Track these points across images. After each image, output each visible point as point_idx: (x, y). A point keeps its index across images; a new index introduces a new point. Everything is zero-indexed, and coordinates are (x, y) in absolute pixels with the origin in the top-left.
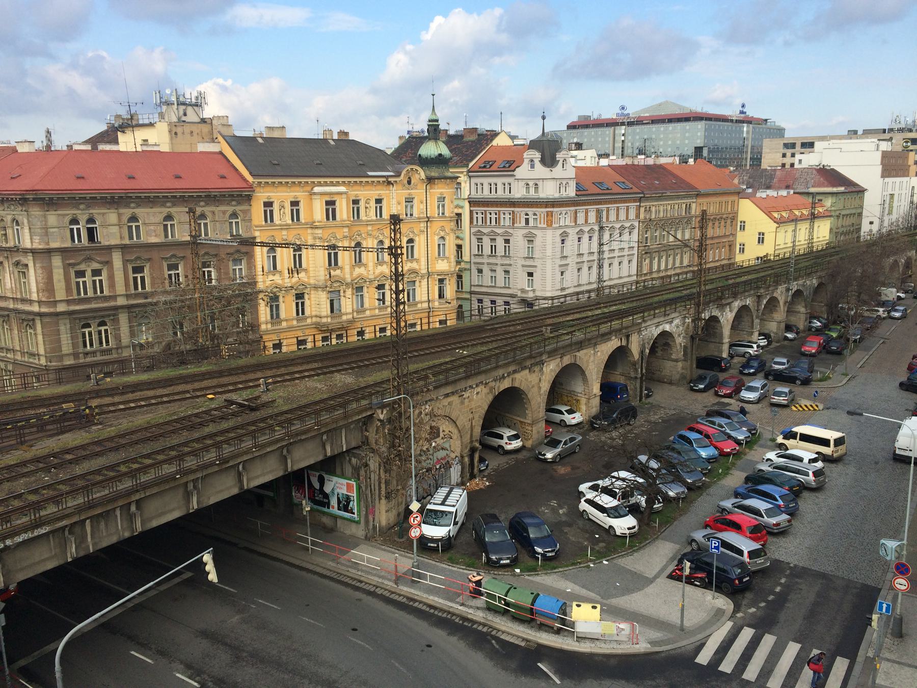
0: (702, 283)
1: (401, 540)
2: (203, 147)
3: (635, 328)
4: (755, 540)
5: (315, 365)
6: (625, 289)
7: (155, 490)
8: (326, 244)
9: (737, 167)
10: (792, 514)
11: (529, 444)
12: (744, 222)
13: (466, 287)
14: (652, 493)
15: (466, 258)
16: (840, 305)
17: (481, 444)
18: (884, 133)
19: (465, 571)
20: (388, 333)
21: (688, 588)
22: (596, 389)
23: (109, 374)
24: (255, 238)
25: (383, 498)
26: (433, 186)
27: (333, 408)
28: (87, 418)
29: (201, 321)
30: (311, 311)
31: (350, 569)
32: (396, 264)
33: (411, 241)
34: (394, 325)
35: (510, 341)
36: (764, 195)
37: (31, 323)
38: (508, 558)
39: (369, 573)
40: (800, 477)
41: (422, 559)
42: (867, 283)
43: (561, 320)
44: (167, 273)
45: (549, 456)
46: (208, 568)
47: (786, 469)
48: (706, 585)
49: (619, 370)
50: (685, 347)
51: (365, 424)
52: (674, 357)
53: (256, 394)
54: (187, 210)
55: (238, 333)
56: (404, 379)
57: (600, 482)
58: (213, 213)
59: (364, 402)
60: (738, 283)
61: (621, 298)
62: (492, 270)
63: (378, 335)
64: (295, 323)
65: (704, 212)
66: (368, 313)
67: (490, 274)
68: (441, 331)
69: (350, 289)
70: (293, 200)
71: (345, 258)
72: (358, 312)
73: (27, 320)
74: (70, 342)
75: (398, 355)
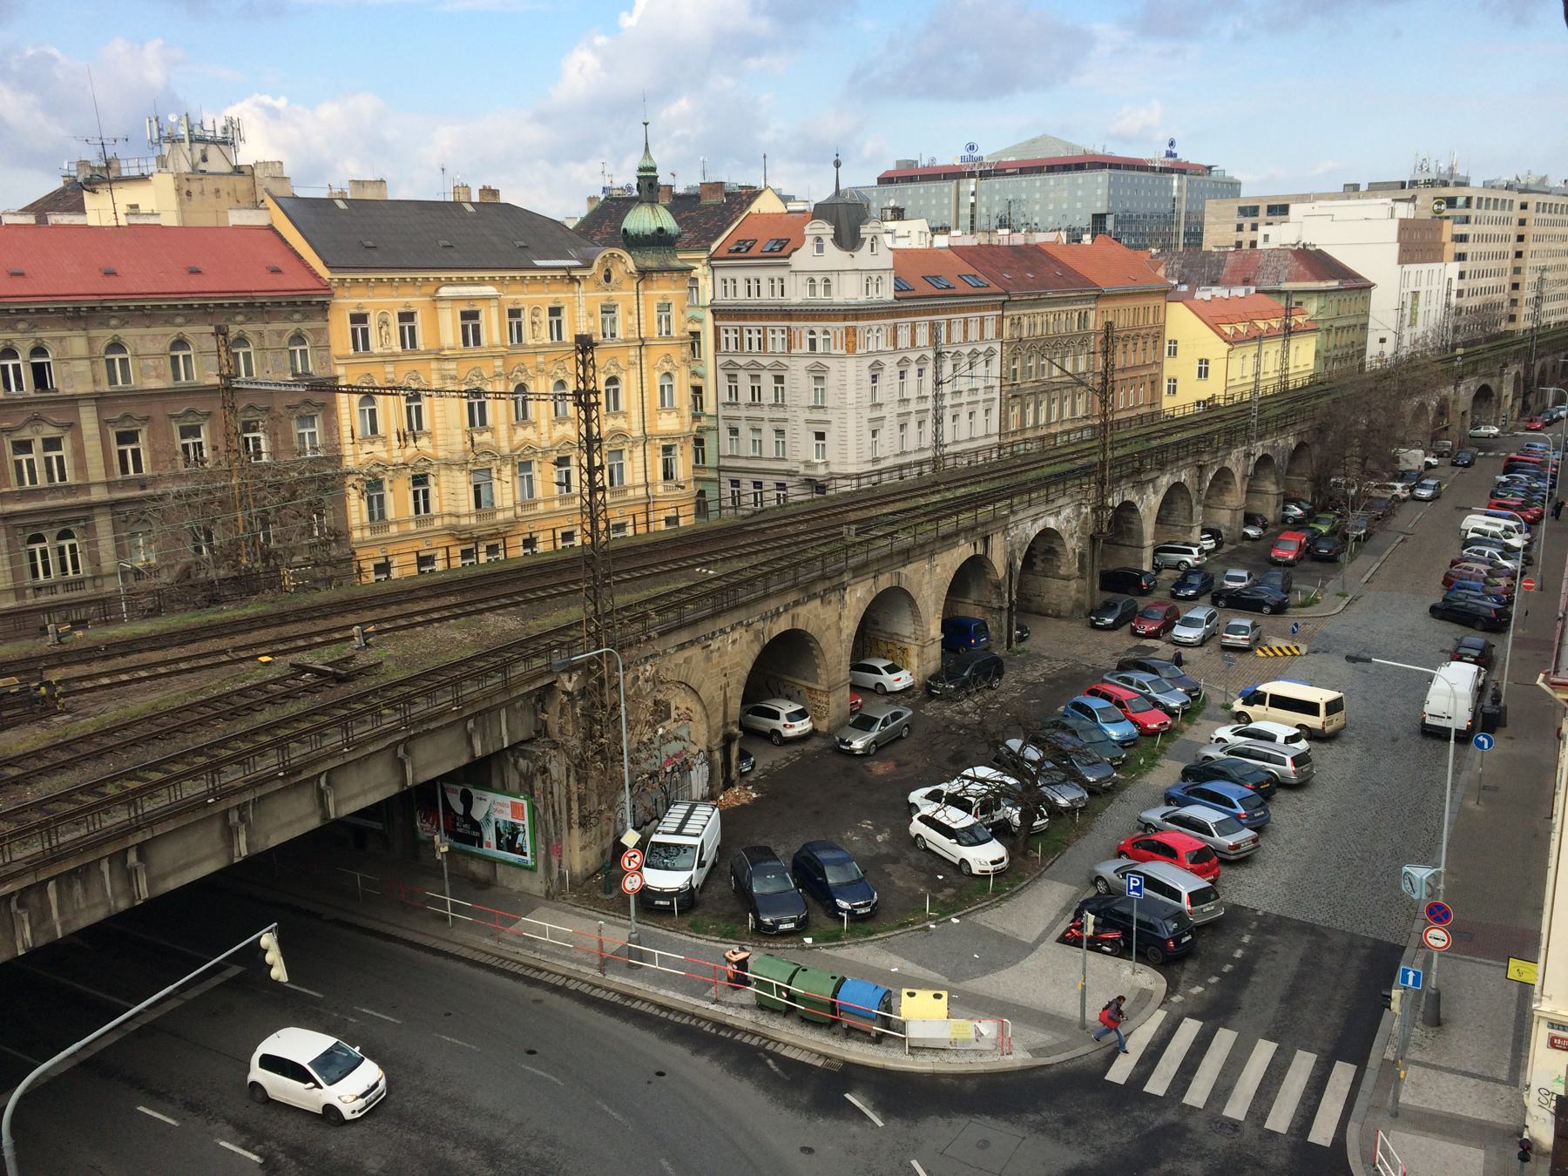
0: (1108, 446)
1: (609, 897)
2: (238, 218)
4: (1200, 873)
5: (452, 600)
6: (980, 458)
7: (171, 826)
8: (464, 388)
9: (1163, 248)
10: (1260, 828)
11: (823, 726)
12: (1176, 342)
13: (711, 460)
14: (1031, 801)
15: (709, 408)
16: (1333, 480)
17: (741, 727)
18: (1402, 189)
19: (719, 945)
20: (578, 542)
21: (1093, 957)
22: (935, 630)
23: (80, 624)
24: (336, 378)
25: (576, 826)
26: (650, 284)
27: (485, 674)
28: (44, 702)
29: (245, 528)
30: (441, 506)
31: (520, 950)
32: (588, 421)
33: (612, 380)
34: (588, 527)
35: (787, 551)
36: (1207, 296)
38: (792, 921)
39: (559, 957)
40: (1272, 767)
41: (645, 927)
42: (1376, 441)
43: (874, 512)
44: (179, 443)
45: (858, 744)
46: (269, 958)
47: (1248, 754)
48: (1122, 952)
49: (974, 596)
50: (1082, 556)
51: (540, 699)
52: (1063, 571)
53: (347, 652)
54: (212, 329)
55: (312, 546)
56: (607, 621)
57: (944, 787)
58: (261, 334)
59: (538, 663)
60: (1167, 446)
61: (974, 474)
62: (754, 430)
63: (560, 544)
64: (412, 526)
65: (1109, 326)
66: (541, 507)
67: (751, 436)
68: (669, 536)
69: (509, 467)
70: (403, 310)
71: (498, 412)
72: (523, 506)
74: (8, 568)
75: (595, 578)
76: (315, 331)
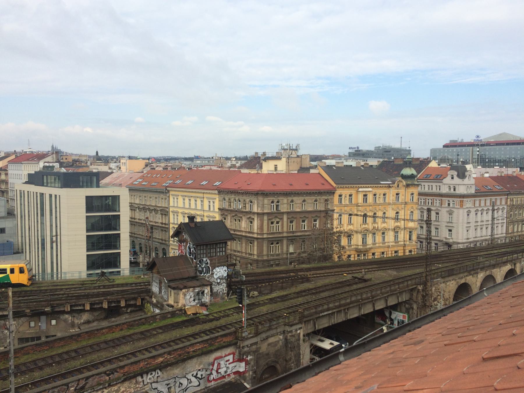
3: (519, 260)
37: (252, 242)
58: (320, 199)
73: (250, 240)
76: (331, 199)
